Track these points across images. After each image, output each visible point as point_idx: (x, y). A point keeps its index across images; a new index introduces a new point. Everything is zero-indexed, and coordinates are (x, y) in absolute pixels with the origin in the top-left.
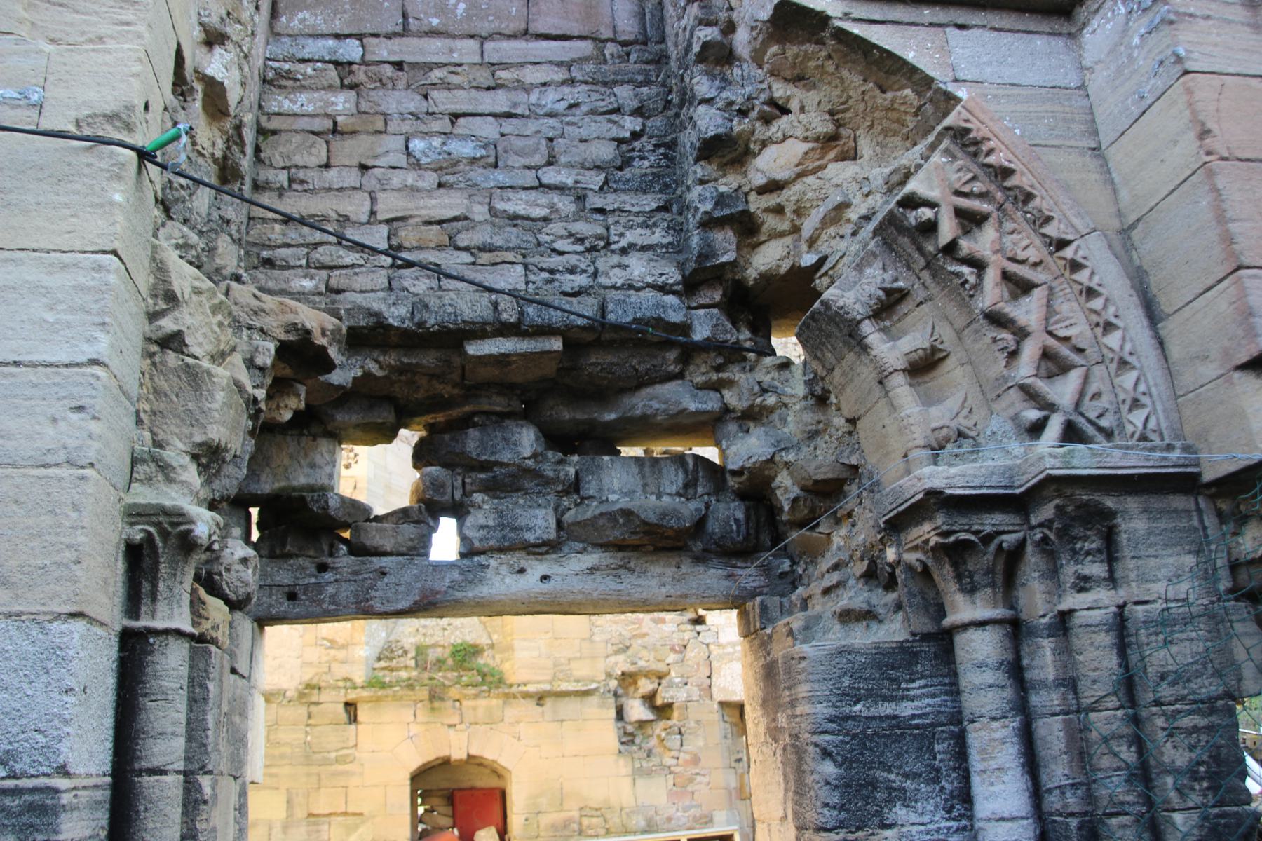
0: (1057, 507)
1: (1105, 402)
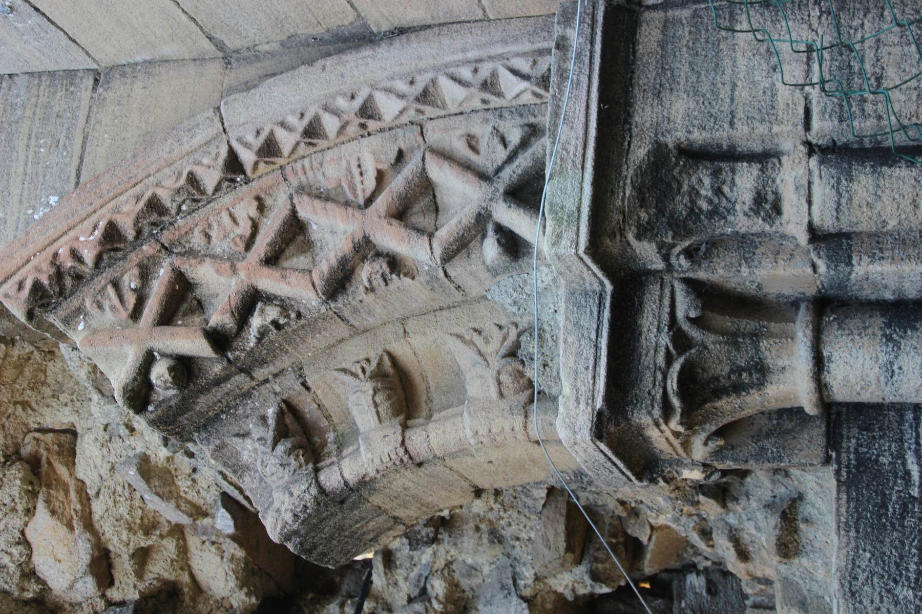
0: (639, 237)
1: (482, 131)
